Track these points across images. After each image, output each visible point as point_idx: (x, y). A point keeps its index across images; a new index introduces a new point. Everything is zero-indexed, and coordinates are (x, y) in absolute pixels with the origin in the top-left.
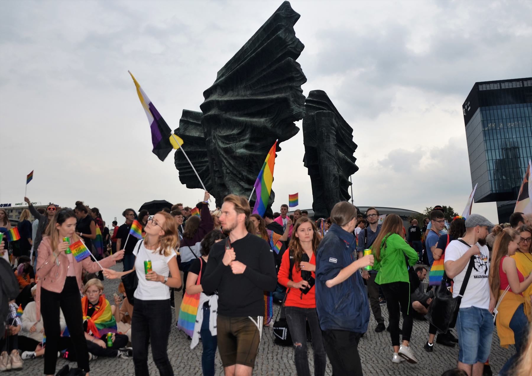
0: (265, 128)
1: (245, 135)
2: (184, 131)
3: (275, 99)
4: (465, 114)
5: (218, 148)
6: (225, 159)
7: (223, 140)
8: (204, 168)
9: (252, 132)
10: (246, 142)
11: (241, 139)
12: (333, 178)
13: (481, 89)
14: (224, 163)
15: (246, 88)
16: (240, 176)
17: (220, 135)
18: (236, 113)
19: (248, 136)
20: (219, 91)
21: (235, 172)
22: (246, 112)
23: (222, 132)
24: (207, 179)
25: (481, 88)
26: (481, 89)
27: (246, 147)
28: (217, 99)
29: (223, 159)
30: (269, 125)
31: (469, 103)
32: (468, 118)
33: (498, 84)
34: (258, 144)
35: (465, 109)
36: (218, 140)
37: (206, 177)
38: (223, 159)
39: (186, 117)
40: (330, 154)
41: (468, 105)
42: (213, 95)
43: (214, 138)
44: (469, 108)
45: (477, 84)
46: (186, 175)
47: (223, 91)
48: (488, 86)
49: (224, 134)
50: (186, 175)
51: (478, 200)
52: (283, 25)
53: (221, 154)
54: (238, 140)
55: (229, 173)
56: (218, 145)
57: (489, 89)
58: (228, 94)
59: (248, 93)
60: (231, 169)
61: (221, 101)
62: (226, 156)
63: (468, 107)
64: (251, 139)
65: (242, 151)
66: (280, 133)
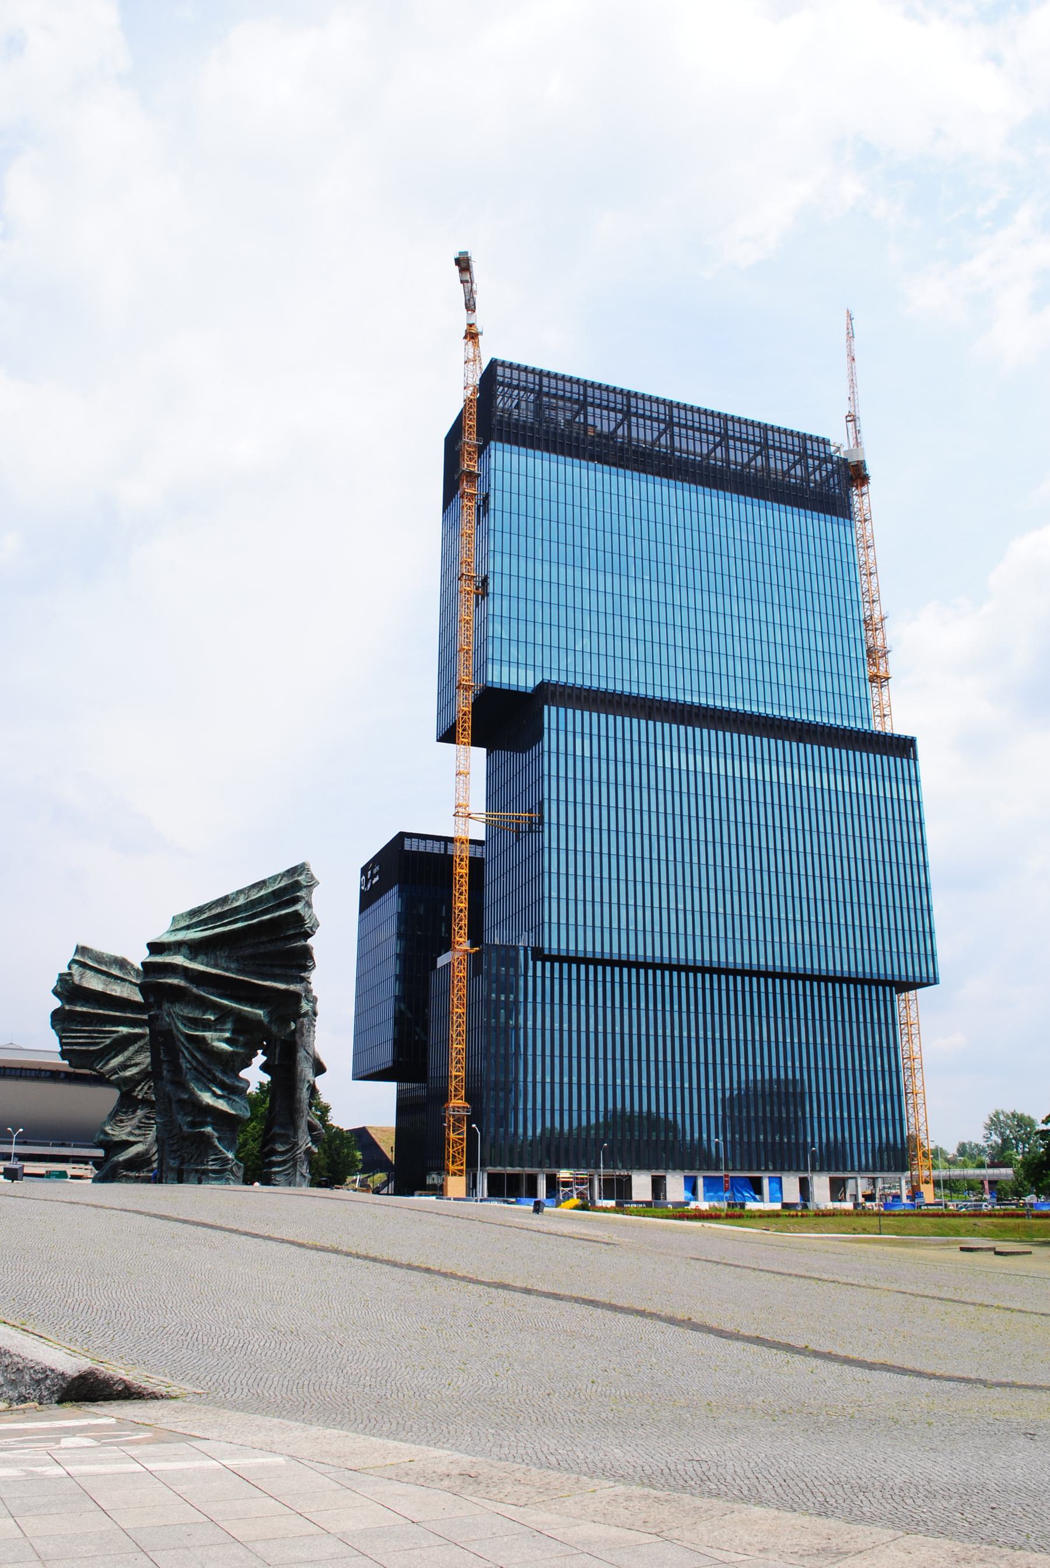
0: (260, 1022)
1: (224, 1023)
2: (80, 979)
4: (363, 888)
5: (175, 1031)
6: (187, 1049)
7: (185, 1022)
8: (108, 1041)
9: (235, 1022)
10: (227, 1035)
11: (218, 1027)
12: (307, 1085)
13: (407, 848)
14: (183, 1053)
15: (229, 958)
16: (210, 1077)
17: (181, 1013)
18: (212, 990)
19: (229, 1026)
20: (184, 950)
21: (201, 1069)
22: (229, 993)
23: (186, 1011)
25: (408, 845)
26: (407, 848)
27: (227, 1041)
29: (183, 1049)
30: (266, 1020)
31: (377, 868)
32: (367, 899)
33: (442, 843)
34: (241, 1039)
35: (366, 878)
36: (177, 1021)
37: (107, 1055)
38: (183, 1049)
39: (83, 955)
40: (308, 1053)
41: (375, 871)
42: (172, 953)
43: (169, 1015)
44: (376, 879)
45: (402, 836)
46: (75, 1047)
47: (191, 953)
48: (422, 843)
49: (190, 1015)
50: (75, 1047)
51: (362, 1075)
52: (303, 898)
53: (180, 1040)
54: (213, 1027)
55: (190, 1069)
56: (178, 1030)
57: (423, 850)
58: (200, 958)
59: (233, 966)
60: (194, 1064)
62: (187, 1045)
63: (373, 876)
64: (234, 1031)
65: (225, 1046)
66: (276, 1030)
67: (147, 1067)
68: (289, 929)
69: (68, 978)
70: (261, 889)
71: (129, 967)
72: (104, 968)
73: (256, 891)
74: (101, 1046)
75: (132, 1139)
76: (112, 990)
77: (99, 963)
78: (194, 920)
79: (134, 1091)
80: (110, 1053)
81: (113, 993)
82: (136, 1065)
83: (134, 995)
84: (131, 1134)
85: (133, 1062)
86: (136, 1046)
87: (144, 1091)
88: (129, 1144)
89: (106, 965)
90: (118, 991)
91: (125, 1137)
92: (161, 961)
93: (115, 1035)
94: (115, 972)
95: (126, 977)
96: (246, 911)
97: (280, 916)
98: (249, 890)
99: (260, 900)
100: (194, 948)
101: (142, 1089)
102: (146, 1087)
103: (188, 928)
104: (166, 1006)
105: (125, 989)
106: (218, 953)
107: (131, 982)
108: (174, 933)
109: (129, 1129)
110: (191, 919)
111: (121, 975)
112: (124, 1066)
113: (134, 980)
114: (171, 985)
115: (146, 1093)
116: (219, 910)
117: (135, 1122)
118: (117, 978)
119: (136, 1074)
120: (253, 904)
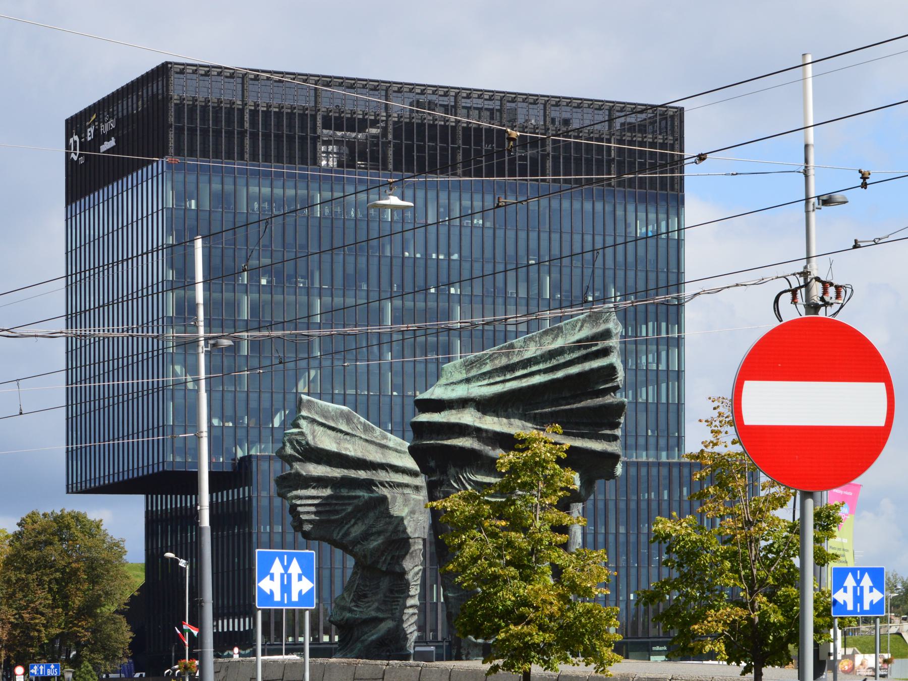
2: (314, 437)
3: (598, 452)
8: (350, 509)
24: (347, 526)
28: (478, 424)
37: (346, 524)
61: (487, 431)
67: (391, 535)
68: (598, 383)
69: (299, 438)
70: (557, 336)
71: (355, 421)
72: (332, 424)
73: (549, 338)
74: (343, 514)
75: (380, 615)
76: (346, 449)
77: (325, 417)
78: (474, 372)
79: (378, 562)
80: (350, 521)
81: (348, 453)
82: (379, 533)
83: (367, 454)
84: (378, 609)
85: (374, 530)
86: (377, 512)
87: (387, 562)
88: (377, 621)
89: (333, 420)
90: (351, 449)
91: (374, 614)
92: (445, 420)
93: (356, 501)
94: (344, 427)
95: (354, 433)
96: (545, 361)
97: (592, 370)
98: (540, 338)
99: (560, 351)
100: (485, 405)
101: (385, 559)
102: (389, 558)
103: (468, 381)
104: (452, 471)
105: (356, 447)
106: (510, 410)
107: (361, 438)
108: (450, 388)
109: (376, 605)
110: (468, 371)
111: (349, 431)
112: (366, 536)
113: (363, 436)
114: (462, 449)
115: (389, 564)
116: (504, 361)
117: (380, 596)
118: (347, 434)
119: (382, 543)
120: (552, 354)
